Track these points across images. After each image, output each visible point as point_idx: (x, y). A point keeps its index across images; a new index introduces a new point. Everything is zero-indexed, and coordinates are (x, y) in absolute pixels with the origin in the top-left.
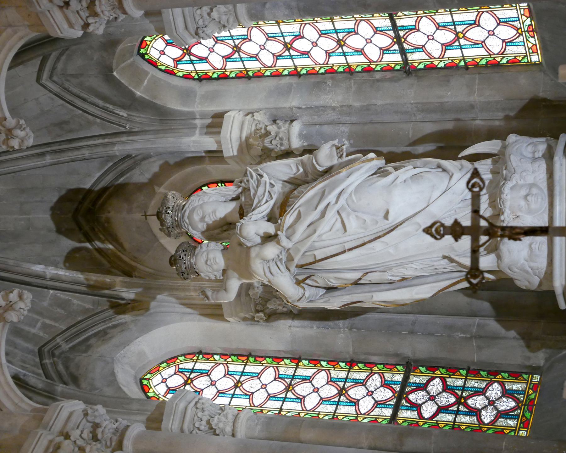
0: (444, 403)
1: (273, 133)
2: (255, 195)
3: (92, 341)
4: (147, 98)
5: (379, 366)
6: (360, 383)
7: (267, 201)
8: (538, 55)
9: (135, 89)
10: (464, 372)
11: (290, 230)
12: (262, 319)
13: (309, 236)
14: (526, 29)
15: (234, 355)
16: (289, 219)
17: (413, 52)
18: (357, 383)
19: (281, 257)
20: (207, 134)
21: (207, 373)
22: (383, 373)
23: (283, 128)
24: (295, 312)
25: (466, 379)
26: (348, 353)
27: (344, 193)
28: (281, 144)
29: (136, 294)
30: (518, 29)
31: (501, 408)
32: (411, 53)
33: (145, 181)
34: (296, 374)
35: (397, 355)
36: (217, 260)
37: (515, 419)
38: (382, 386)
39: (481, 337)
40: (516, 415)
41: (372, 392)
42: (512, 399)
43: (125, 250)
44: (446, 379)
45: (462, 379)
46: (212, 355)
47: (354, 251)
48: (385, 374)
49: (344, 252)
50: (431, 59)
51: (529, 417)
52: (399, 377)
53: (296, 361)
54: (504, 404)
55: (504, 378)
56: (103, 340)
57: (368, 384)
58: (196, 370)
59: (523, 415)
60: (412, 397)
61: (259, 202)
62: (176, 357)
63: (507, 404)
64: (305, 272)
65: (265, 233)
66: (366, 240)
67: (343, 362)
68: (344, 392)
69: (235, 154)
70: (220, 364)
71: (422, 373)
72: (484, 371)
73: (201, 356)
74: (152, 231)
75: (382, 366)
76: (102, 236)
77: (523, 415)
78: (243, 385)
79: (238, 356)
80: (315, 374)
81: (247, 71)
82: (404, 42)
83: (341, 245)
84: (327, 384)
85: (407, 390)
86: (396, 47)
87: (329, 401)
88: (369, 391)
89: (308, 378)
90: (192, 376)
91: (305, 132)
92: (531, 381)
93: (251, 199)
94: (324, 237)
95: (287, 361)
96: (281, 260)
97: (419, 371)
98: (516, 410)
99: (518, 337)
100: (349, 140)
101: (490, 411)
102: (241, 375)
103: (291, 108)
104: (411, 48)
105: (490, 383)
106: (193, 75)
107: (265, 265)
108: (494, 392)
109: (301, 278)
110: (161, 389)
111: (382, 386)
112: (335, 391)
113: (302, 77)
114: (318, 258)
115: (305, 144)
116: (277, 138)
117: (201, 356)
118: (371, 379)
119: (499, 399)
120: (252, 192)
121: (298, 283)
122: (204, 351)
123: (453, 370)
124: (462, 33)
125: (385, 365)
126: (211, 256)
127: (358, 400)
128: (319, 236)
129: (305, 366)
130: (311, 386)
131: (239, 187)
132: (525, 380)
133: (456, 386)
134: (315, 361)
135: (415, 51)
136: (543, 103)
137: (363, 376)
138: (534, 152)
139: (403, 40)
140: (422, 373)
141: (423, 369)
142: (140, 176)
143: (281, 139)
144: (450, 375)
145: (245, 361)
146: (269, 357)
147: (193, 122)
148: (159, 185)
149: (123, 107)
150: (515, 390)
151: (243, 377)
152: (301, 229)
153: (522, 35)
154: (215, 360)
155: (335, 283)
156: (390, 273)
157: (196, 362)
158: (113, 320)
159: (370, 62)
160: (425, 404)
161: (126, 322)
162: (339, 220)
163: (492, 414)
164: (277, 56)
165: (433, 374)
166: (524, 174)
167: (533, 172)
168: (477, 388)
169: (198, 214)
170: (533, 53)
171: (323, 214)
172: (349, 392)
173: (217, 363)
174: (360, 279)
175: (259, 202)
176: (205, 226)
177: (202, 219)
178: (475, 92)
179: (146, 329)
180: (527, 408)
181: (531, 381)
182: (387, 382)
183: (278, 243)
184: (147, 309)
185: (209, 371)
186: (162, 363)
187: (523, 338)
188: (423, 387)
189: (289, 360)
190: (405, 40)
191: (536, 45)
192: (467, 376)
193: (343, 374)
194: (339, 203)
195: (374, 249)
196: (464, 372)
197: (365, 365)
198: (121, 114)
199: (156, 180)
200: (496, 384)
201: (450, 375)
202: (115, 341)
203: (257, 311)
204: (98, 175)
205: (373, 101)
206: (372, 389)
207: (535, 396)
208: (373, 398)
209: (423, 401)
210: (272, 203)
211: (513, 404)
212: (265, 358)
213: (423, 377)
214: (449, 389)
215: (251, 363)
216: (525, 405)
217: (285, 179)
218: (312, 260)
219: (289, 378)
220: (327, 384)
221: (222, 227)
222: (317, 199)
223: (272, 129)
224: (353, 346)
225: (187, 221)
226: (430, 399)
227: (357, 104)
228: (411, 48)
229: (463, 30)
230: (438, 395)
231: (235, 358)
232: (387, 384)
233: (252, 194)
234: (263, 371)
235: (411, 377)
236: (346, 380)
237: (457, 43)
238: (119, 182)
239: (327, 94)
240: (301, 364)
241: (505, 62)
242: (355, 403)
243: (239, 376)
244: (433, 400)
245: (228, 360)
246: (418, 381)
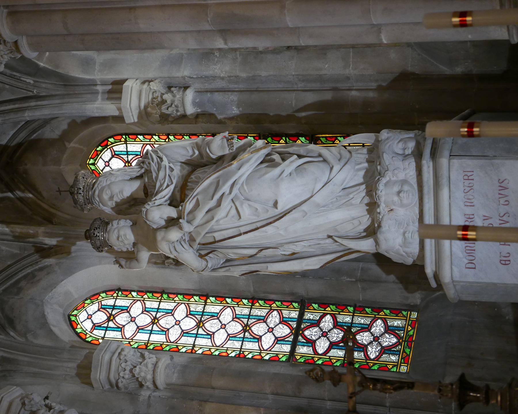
0: (335, 339)
1: (169, 102)
2: (157, 178)
3: (23, 284)
4: (50, 68)
5: (277, 303)
6: (262, 320)
7: (168, 186)
9: (38, 60)
10: (351, 309)
11: (191, 216)
12: (171, 264)
13: (208, 222)
15: (150, 292)
16: (189, 206)
18: (259, 320)
19: (184, 238)
20: (108, 99)
21: (127, 310)
22: (280, 310)
23: (178, 96)
25: (353, 316)
27: (237, 184)
28: (177, 111)
29: (57, 241)
31: (385, 344)
33: (57, 137)
34: (205, 311)
35: (292, 294)
36: (128, 237)
37: (397, 355)
38: (280, 323)
39: (364, 281)
40: (397, 351)
41: (273, 329)
42: (394, 335)
43: (44, 198)
44: (336, 315)
45: (350, 315)
46: (130, 291)
47: (249, 234)
48: (283, 311)
49: (240, 235)
51: (408, 353)
52: (295, 314)
53: (204, 298)
54: (387, 340)
55: (386, 315)
56: (32, 283)
57: (268, 321)
58: (117, 306)
59: (404, 351)
60: (307, 333)
61: (161, 185)
62: (99, 294)
63: (389, 340)
64: (207, 249)
65: (168, 217)
66: (259, 225)
67: (245, 299)
68: (248, 328)
69: (136, 120)
71: (315, 309)
72: (368, 308)
73: (120, 293)
74: (67, 182)
76: (22, 187)
77: (404, 351)
78: (160, 322)
79: (152, 292)
80: (222, 311)
83: (237, 229)
84: (233, 320)
85: (302, 326)
87: (235, 337)
88: (270, 328)
89: (216, 315)
90: (114, 313)
91: (197, 101)
92: (410, 318)
93: (153, 181)
94: (221, 222)
95: (197, 298)
96: (184, 240)
98: (397, 346)
99: (397, 281)
100: (239, 108)
101: (374, 347)
102: (157, 312)
103: (183, 78)
105: (375, 320)
107: (170, 245)
108: (378, 329)
109: (203, 252)
110: (88, 325)
111: (280, 323)
112: (240, 328)
114: (217, 239)
115: (199, 110)
116: (173, 106)
117: (120, 293)
118: (270, 316)
119: (382, 335)
120: (154, 175)
121: (201, 256)
122: (122, 288)
123: (342, 307)
125: (282, 302)
126: (122, 233)
127: (261, 337)
128: (217, 221)
129: (212, 303)
130: (219, 323)
131: (142, 168)
132: (405, 317)
133: (345, 323)
134: (221, 298)
137: (263, 313)
138: (404, 149)
140: (315, 309)
141: (316, 306)
142: (51, 133)
143: (177, 106)
144: (339, 312)
145: (160, 298)
146: (181, 294)
147: (95, 88)
148: (70, 142)
149: (29, 74)
150: (396, 327)
151: (158, 313)
152: (200, 216)
154: (133, 297)
155: (233, 256)
156: (281, 249)
157: (116, 299)
158: (39, 263)
160: (319, 340)
161: (51, 265)
162: (234, 207)
163: (377, 350)
165: (325, 310)
166: (396, 172)
167: (404, 169)
168: (363, 324)
169: (107, 194)
171: (219, 204)
172: (253, 329)
173: (135, 300)
174: (256, 255)
175: (161, 185)
176: (114, 204)
177: (111, 198)
179: (70, 272)
180: (407, 344)
181: (410, 318)
182: (284, 319)
183: (181, 228)
184: (69, 253)
185: (128, 307)
186: (86, 300)
187: (401, 282)
188: (316, 324)
189: (198, 297)
192: (354, 313)
193: (246, 311)
194: (232, 193)
195: (266, 232)
196: (351, 309)
197: (265, 302)
198: (28, 81)
199: (65, 137)
200: (379, 320)
201: (339, 312)
202: (43, 283)
204: (12, 133)
206: (272, 325)
207: (414, 333)
208: (274, 334)
209: (317, 337)
210: (172, 187)
211: (394, 340)
212: (177, 294)
213: (316, 314)
214: (339, 326)
215: (165, 299)
216: (405, 341)
217: (183, 161)
218: (212, 240)
219: (199, 315)
220: (233, 320)
222: (213, 188)
223: (168, 97)
225: (97, 199)
226: (323, 336)
227: (244, 75)
230: (329, 331)
231: (150, 295)
232: (285, 321)
233: (154, 177)
234: (176, 308)
235: (306, 313)
236: (249, 316)
238: (32, 137)
239: (215, 65)
240: (208, 301)
242: (258, 339)
243: (155, 313)
244: (326, 336)
245: (144, 297)
246: (312, 317)
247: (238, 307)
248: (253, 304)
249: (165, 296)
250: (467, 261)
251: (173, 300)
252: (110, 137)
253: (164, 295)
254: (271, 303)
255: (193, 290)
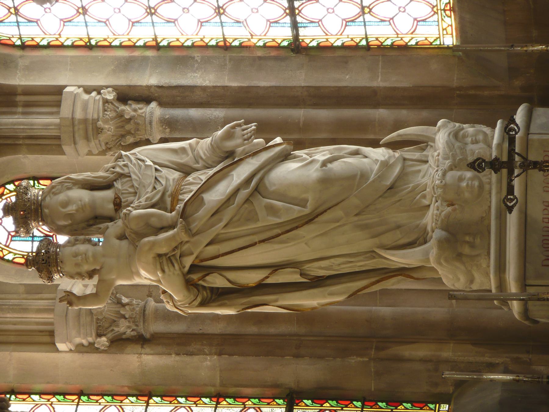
5: (253, 400)
8: (453, 37)
10: (359, 404)
14: (442, 8)
15: (60, 394)
17: (307, 27)
22: (259, 408)
24: (148, 336)
26: (214, 386)
30: (434, 7)
32: (304, 27)
35: (276, 386)
48: (262, 409)
50: (327, 35)
70: (42, 405)
71: (307, 406)
75: (257, 400)
81: (90, 39)
82: (298, 14)
86: (288, 19)
95: (134, 399)
97: (303, 404)
103: (149, 87)
104: (305, 21)
106: (14, 40)
113: (162, 50)
122: (16, 390)
124: (368, 7)
125: (259, 399)
135: (309, 25)
136: (458, 92)
139: (297, 11)
140: (307, 406)
141: (309, 402)
144: (342, 408)
145: (77, 401)
146: (108, 395)
153: (437, 13)
154: (34, 401)
159: (252, 35)
164: (133, 23)
165: (322, 406)
170: (447, 34)
173: (37, 405)
178: (378, 77)
190: (300, 11)
191: (451, 26)
197: (235, 400)
201: (342, 408)
203: (99, 335)
205: (255, 82)
215: (84, 402)
221: (88, 221)
224: (220, 377)
228: (305, 21)
229: (370, 5)
231: (61, 398)
237: (361, 19)
239: (195, 72)
240: (151, 401)
241: (414, 43)
245: (51, 400)
247: (196, 406)
248: (218, 403)
249: (84, 398)
250: (544, 258)
251: (97, 402)
252: (9, 183)
253: (82, 397)
254: (244, 400)
255: (128, 387)
